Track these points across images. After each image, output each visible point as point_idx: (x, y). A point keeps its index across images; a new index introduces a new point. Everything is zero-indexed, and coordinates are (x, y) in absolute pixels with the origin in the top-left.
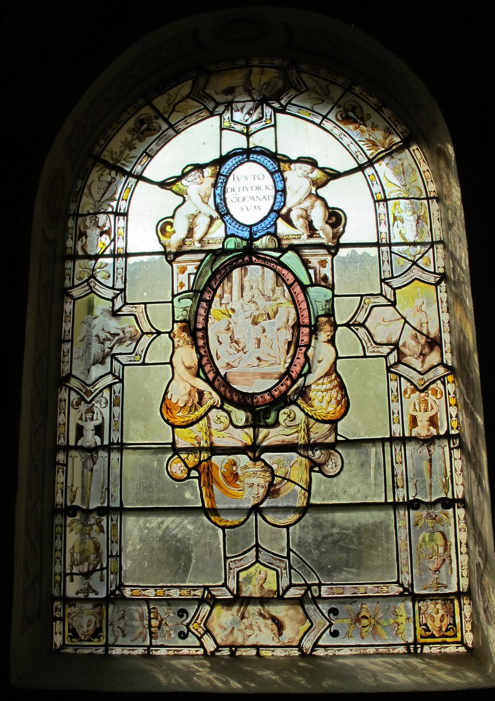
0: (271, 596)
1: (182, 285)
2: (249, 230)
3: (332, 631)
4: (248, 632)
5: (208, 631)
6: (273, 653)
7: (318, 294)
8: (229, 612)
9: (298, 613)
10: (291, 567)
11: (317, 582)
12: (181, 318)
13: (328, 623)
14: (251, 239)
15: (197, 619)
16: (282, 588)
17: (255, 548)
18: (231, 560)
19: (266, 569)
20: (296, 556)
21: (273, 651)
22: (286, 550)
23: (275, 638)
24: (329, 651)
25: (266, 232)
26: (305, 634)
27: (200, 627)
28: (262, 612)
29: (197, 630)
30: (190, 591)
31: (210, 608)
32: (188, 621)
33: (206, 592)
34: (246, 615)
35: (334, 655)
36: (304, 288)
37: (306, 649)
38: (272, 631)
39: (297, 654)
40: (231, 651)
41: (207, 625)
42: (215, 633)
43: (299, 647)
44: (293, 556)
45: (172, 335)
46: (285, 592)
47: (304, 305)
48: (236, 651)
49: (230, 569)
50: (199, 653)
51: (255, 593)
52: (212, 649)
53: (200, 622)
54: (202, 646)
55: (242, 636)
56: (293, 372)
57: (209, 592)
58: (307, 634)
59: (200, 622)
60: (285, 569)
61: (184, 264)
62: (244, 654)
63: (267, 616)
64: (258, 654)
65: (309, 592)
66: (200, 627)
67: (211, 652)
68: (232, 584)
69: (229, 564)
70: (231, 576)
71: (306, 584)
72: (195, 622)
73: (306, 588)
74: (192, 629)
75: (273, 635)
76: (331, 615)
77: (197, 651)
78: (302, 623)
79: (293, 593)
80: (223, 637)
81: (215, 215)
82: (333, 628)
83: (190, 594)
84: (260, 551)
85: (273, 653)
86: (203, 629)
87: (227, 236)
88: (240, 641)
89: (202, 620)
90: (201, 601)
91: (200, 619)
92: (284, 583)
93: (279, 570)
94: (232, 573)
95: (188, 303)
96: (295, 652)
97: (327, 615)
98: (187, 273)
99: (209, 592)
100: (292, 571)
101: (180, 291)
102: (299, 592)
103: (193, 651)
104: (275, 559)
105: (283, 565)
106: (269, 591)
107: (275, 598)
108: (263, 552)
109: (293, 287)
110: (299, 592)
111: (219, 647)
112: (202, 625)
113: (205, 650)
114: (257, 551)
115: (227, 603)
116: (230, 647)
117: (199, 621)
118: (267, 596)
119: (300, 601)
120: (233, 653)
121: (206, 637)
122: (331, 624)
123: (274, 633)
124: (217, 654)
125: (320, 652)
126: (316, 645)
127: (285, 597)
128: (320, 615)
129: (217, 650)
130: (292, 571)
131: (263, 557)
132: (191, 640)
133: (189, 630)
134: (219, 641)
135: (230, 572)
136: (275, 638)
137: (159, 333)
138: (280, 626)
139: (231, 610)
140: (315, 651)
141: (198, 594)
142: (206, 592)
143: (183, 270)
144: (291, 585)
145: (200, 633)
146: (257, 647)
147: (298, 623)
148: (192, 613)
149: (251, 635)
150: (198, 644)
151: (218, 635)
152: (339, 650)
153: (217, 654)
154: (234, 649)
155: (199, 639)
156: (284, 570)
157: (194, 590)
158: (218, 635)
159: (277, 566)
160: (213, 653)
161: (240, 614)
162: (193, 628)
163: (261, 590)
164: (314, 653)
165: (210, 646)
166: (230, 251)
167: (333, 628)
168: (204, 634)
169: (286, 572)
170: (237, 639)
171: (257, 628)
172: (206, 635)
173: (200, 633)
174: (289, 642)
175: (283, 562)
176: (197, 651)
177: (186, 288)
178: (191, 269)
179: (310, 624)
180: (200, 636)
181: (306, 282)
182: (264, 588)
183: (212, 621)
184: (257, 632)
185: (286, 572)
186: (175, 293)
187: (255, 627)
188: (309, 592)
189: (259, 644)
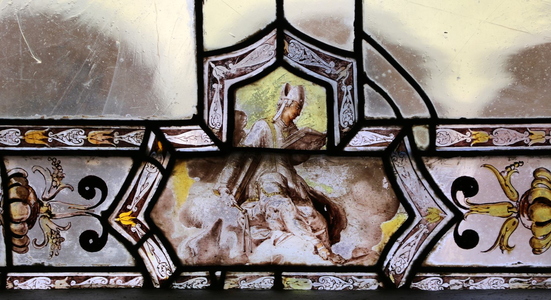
0: (313, 146)
3: (460, 233)
4: (256, 233)
5: (155, 231)
6: (315, 285)
8: (209, 185)
9: (378, 188)
10: (363, 79)
11: (426, 114)
13: (450, 215)
15: (129, 201)
16: (341, 128)
17: (274, 32)
18: (214, 59)
19: (300, 81)
20: (376, 52)
21: (315, 279)
22: (352, 36)
23: (321, 248)
24: (452, 282)
26: (394, 238)
27: (136, 221)
28: (291, 185)
29: (127, 228)
30: (112, 134)
31: (160, 176)
32: (105, 206)
33: (153, 136)
34: (252, 192)
35: (465, 290)
37: (395, 276)
38: (314, 231)
39: (375, 287)
40: (211, 278)
41: (153, 215)
42: (173, 237)
43: (379, 269)
44: (369, 51)
46: (347, 137)
48: (223, 278)
49: (213, 80)
50: (133, 283)
51: (274, 139)
52: (166, 275)
53: (135, 210)
54: (140, 266)
55: (239, 242)
57: (160, 137)
58: (400, 239)
59: (135, 210)
60: (349, 82)
62: (244, 285)
63: (303, 196)
64: (278, 285)
65: (406, 139)
66: (136, 221)
67: (161, 282)
68: (217, 118)
69: (211, 69)
70: (217, 97)
71: (399, 120)
72: (125, 209)
73: (398, 129)
74: (116, 226)
75: (316, 241)
76: (460, 195)
77: (127, 279)
78: (390, 214)
79: (365, 139)
80: (193, 245)
82: (463, 227)
83: (111, 140)
84: (289, 39)
85: (315, 285)
86: (143, 227)
88: (235, 255)
89: (140, 206)
90: (140, 157)
91: (135, 201)
92: (346, 117)
93: (334, 84)
94: (217, 90)
96: (369, 282)
97: (448, 195)
99: (160, 137)
100: (366, 87)
102: (380, 138)
103: (117, 280)
104: (325, 58)
105: (344, 73)
106: (307, 134)
107: (323, 152)
108: (296, 40)
110: (380, 138)
111: (181, 269)
112: (141, 218)
113: (147, 276)
114: (281, 40)
115: (205, 165)
116: (208, 268)
117: (132, 207)
118: (302, 146)
119: (382, 162)
120: (216, 284)
121: (150, 244)
122: (458, 218)
123: (319, 237)
124: (176, 285)
125: (430, 283)
126: (420, 267)
127: (347, 149)
128: (432, 192)
129: (176, 277)
130: (366, 87)
131: (295, 51)
132: (113, 252)
133: (108, 229)
134: (182, 254)
135: (212, 89)
136: (321, 248)
138: (332, 220)
139: (213, 180)
140: (419, 279)
141: (133, 142)
142: (153, 136)
144: (362, 122)
145: (134, 235)
146: (276, 268)
147: (379, 212)
148: (114, 189)
149: (261, 241)
150: (129, 261)
151: (180, 240)
152: (476, 279)
153: (176, 285)
154: (218, 273)
155: (133, 250)
156: (347, 84)
157: (122, 132)
158: (180, 240)
159: (329, 76)
160: (166, 284)
161: (235, 191)
162: (119, 223)
163: (290, 131)
164: (413, 285)
165: (158, 263)
167: (463, 227)
168: (145, 239)
169: (352, 91)
170: (228, 249)
171: (277, 225)
172: (150, 240)
173: (134, 235)
174: (353, 259)
175: (345, 64)
176: (127, 279)
179: (405, 217)
180: (134, 242)
182: (296, 128)
183: (166, 207)
184: (277, 234)
185: (352, 91)
187: (272, 223)
188: (406, 139)
189: (282, 262)
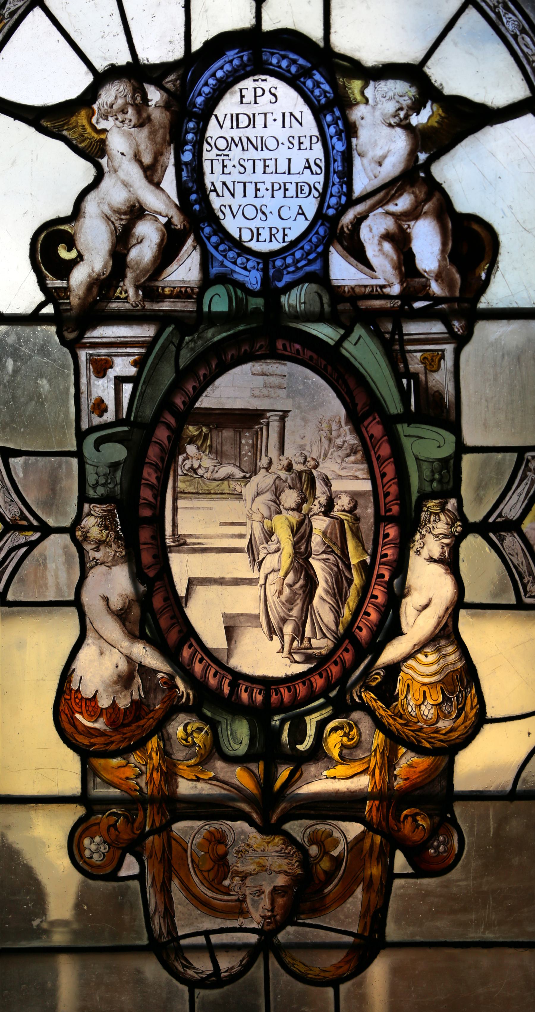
1: (99, 407)
2: (261, 266)
7: (426, 445)
12: (101, 491)
14: (271, 292)
25: (300, 274)
36: (390, 423)
45: (78, 533)
47: (390, 470)
56: (360, 629)
61: (104, 351)
81: (178, 221)
87: (207, 280)
95: (117, 452)
98: (112, 373)
101: (97, 420)
109: (366, 423)
137: (46, 531)
143: (101, 368)
166: (215, 319)
177: (109, 416)
178: (123, 366)
181: (394, 406)
186: (85, 426)
